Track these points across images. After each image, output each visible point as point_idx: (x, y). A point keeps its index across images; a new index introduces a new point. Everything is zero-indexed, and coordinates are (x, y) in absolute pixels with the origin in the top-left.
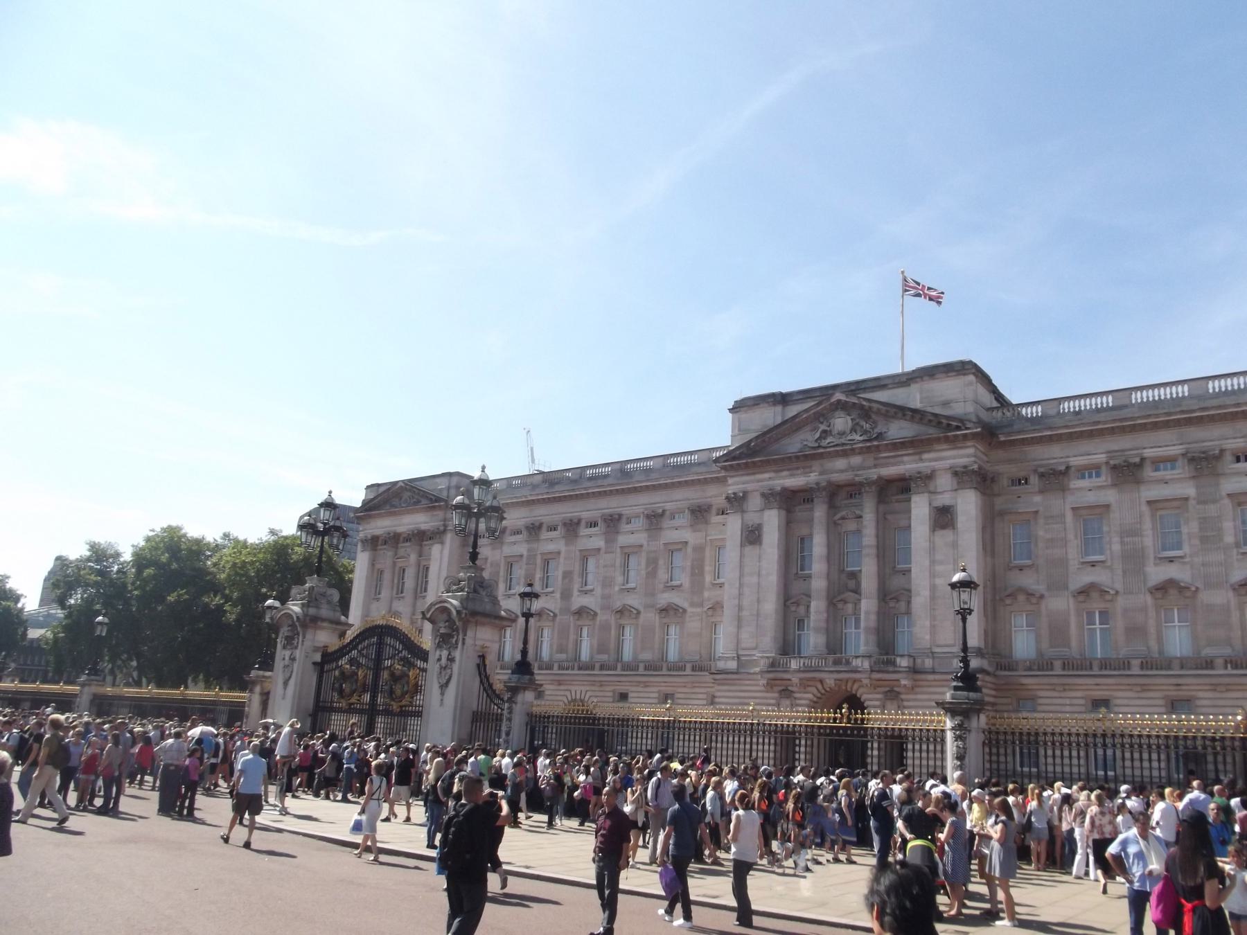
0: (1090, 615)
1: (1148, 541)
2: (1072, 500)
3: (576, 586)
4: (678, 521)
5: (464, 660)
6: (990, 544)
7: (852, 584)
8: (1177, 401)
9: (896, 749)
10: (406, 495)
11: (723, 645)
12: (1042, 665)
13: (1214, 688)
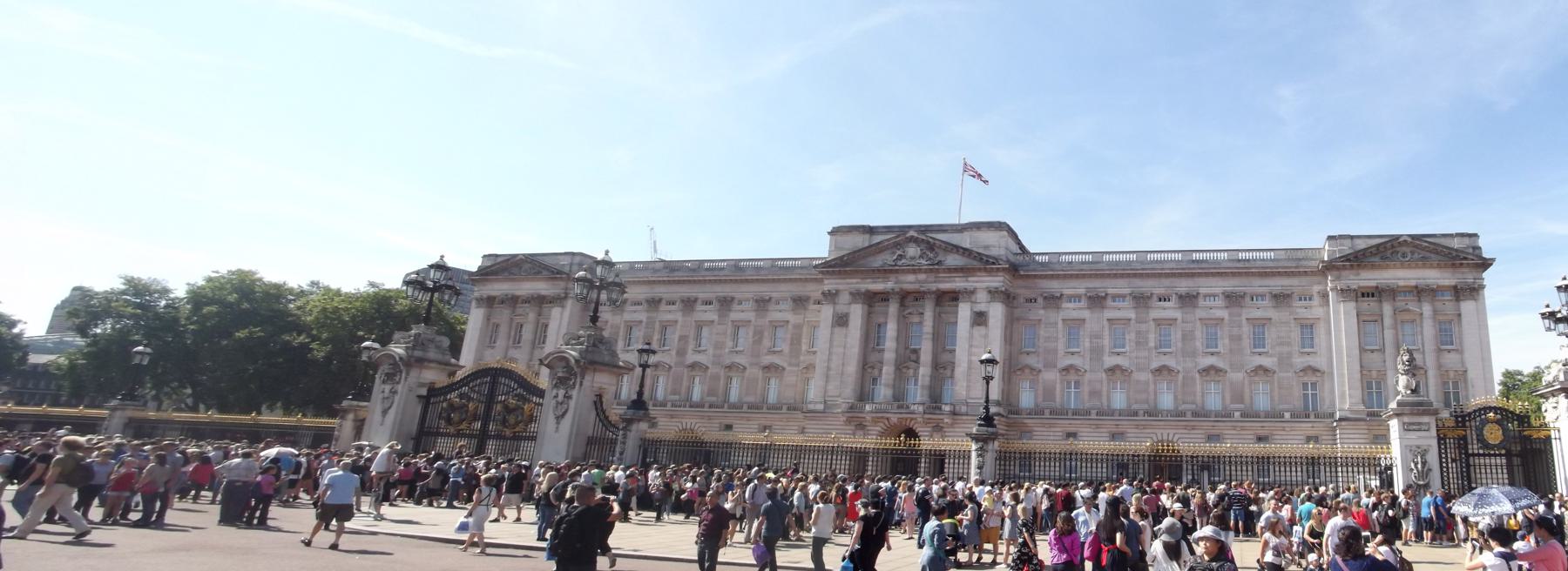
0: (1069, 383)
1: (1106, 342)
2: (1062, 315)
3: (691, 346)
4: (781, 306)
5: (580, 397)
6: (1009, 338)
7: (913, 357)
8: (1130, 262)
9: (938, 463)
10: (527, 266)
11: (814, 393)
12: (1037, 412)
13: (1137, 427)
